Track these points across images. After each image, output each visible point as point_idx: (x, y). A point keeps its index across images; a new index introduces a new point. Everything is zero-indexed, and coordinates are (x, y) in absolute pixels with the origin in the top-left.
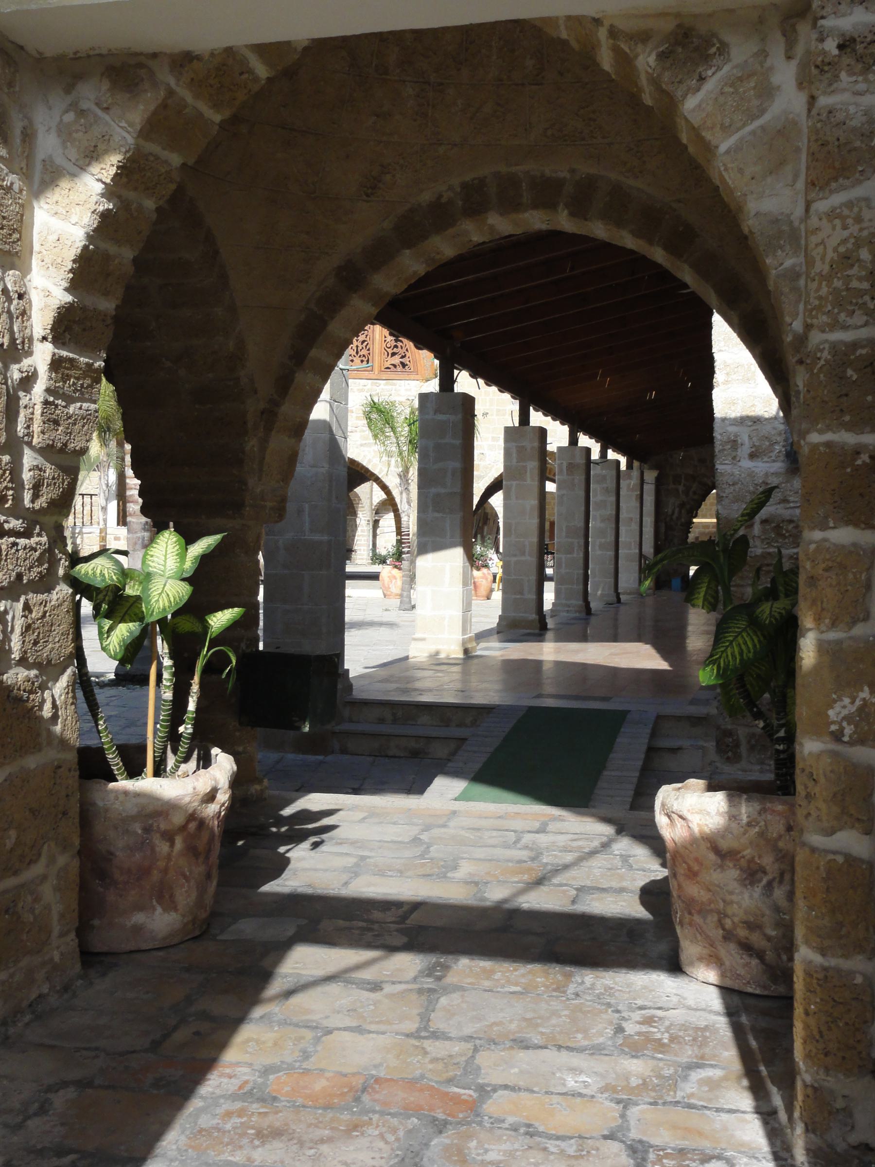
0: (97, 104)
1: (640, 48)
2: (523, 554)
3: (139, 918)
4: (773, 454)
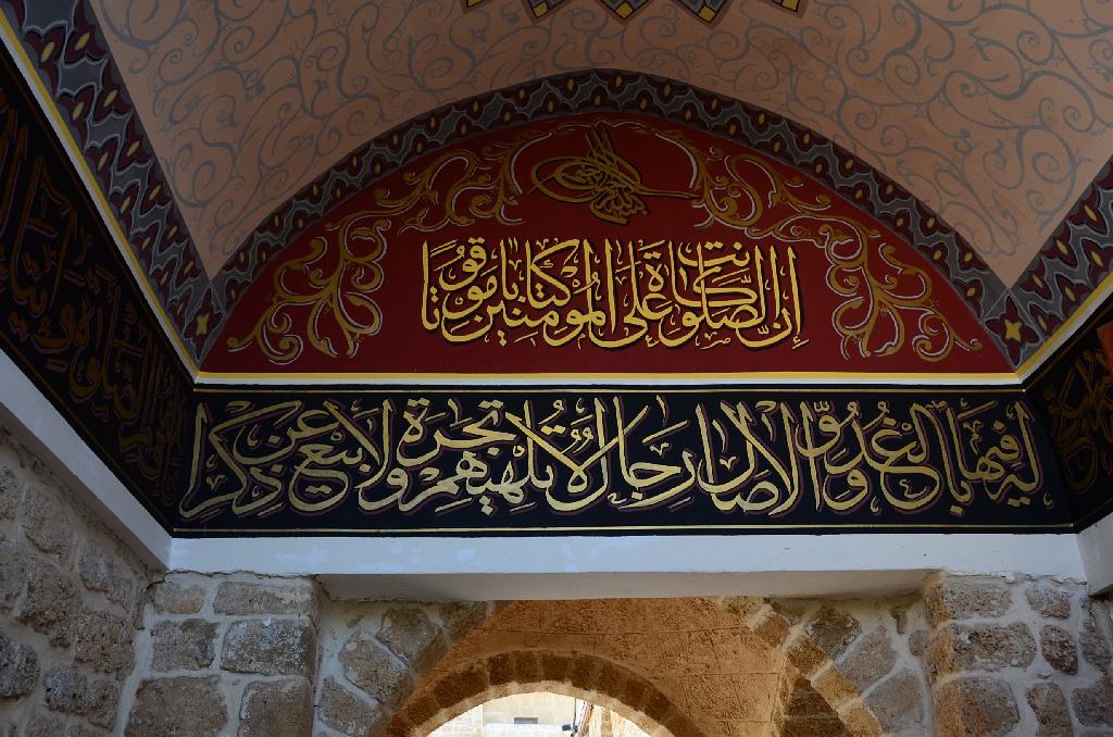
0: (379, 639)
1: (797, 619)
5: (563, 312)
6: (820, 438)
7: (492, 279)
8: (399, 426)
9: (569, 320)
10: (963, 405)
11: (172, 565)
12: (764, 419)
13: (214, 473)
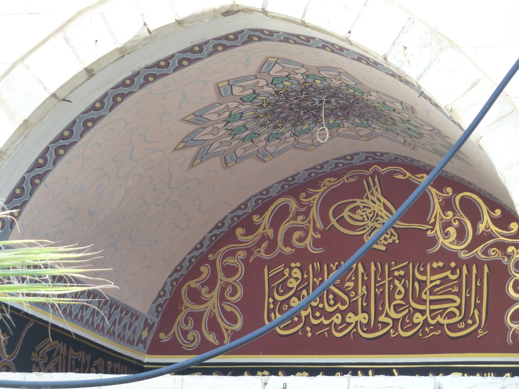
5: (344, 313)
7: (304, 292)
9: (348, 320)
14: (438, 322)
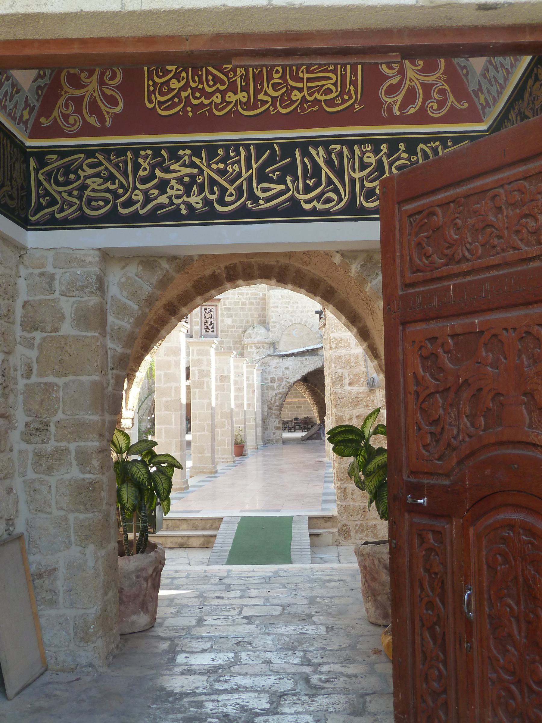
0: (137, 275)
1: (353, 262)
2: (204, 430)
3: (134, 618)
4: (361, 383)
5: (223, 93)
6: (363, 166)
7: (184, 74)
8: (137, 167)
9: (227, 99)
10: (449, 143)
11: (29, 246)
12: (333, 156)
13: (44, 196)
14: (315, 98)
